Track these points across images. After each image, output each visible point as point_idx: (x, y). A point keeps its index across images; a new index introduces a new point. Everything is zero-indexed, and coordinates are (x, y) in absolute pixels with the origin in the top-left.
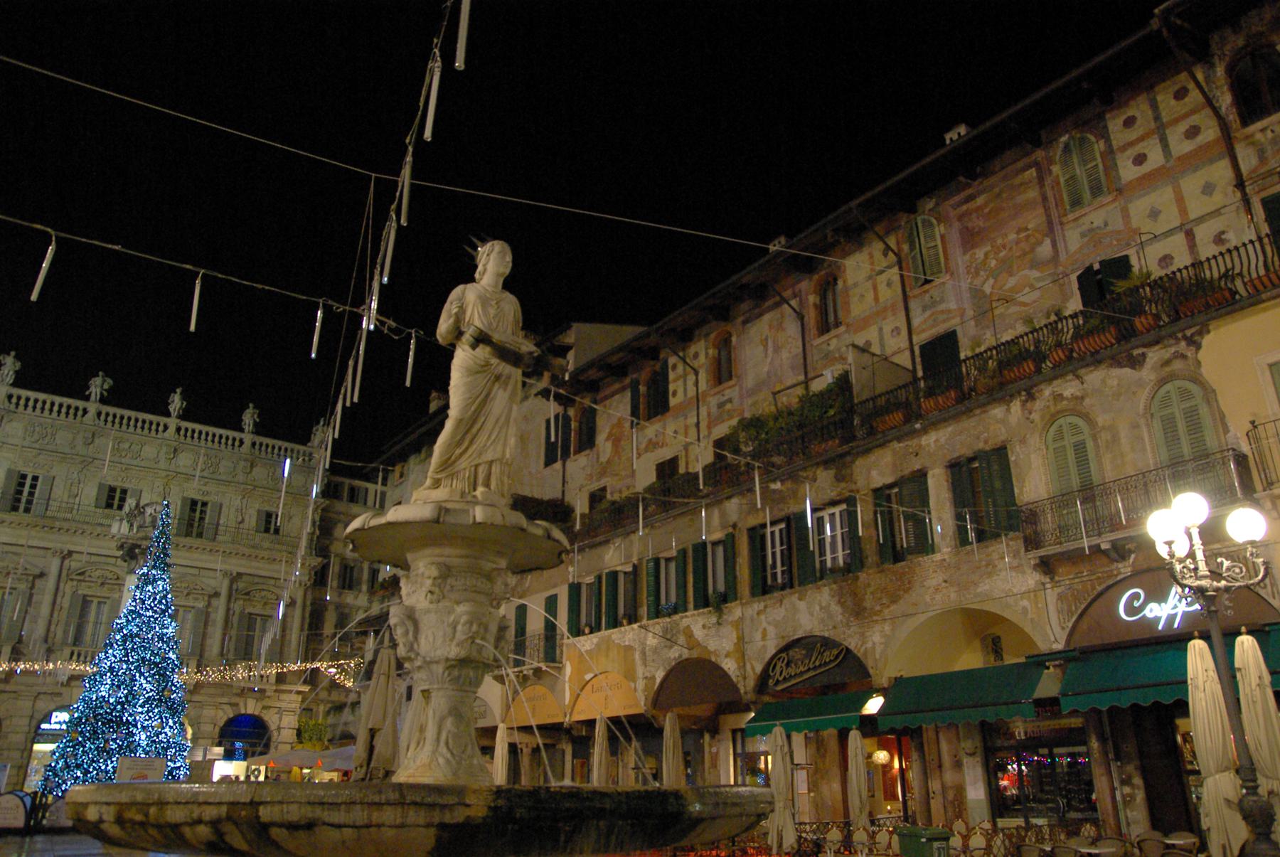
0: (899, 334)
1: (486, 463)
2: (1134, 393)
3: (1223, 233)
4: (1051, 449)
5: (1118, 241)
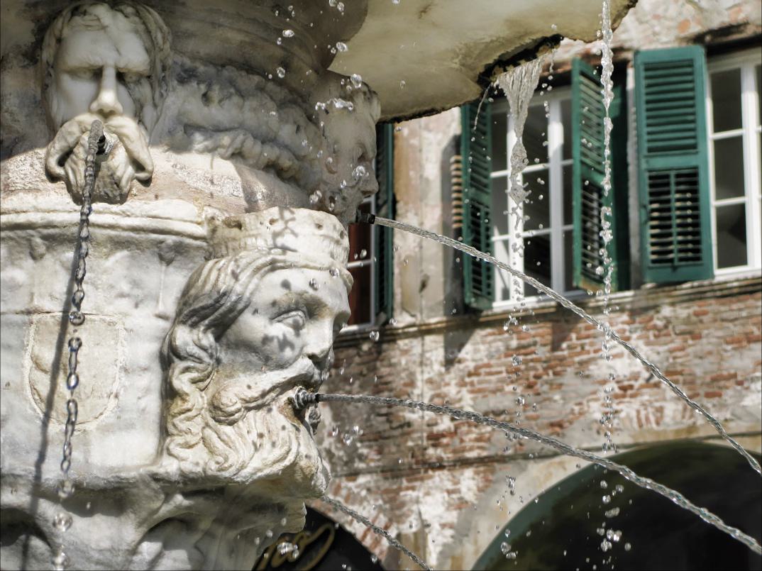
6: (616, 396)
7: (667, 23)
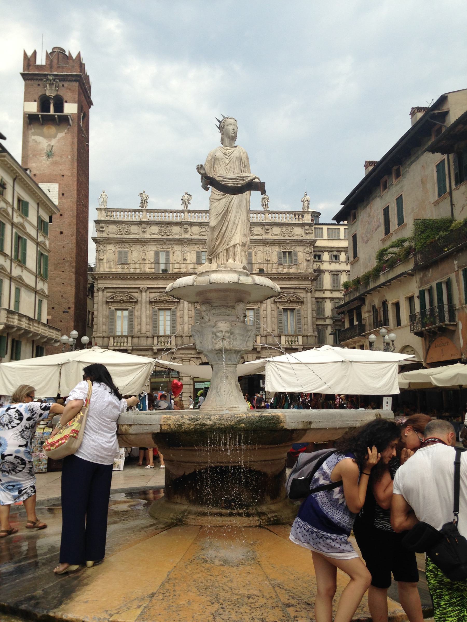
1: (231, 247)
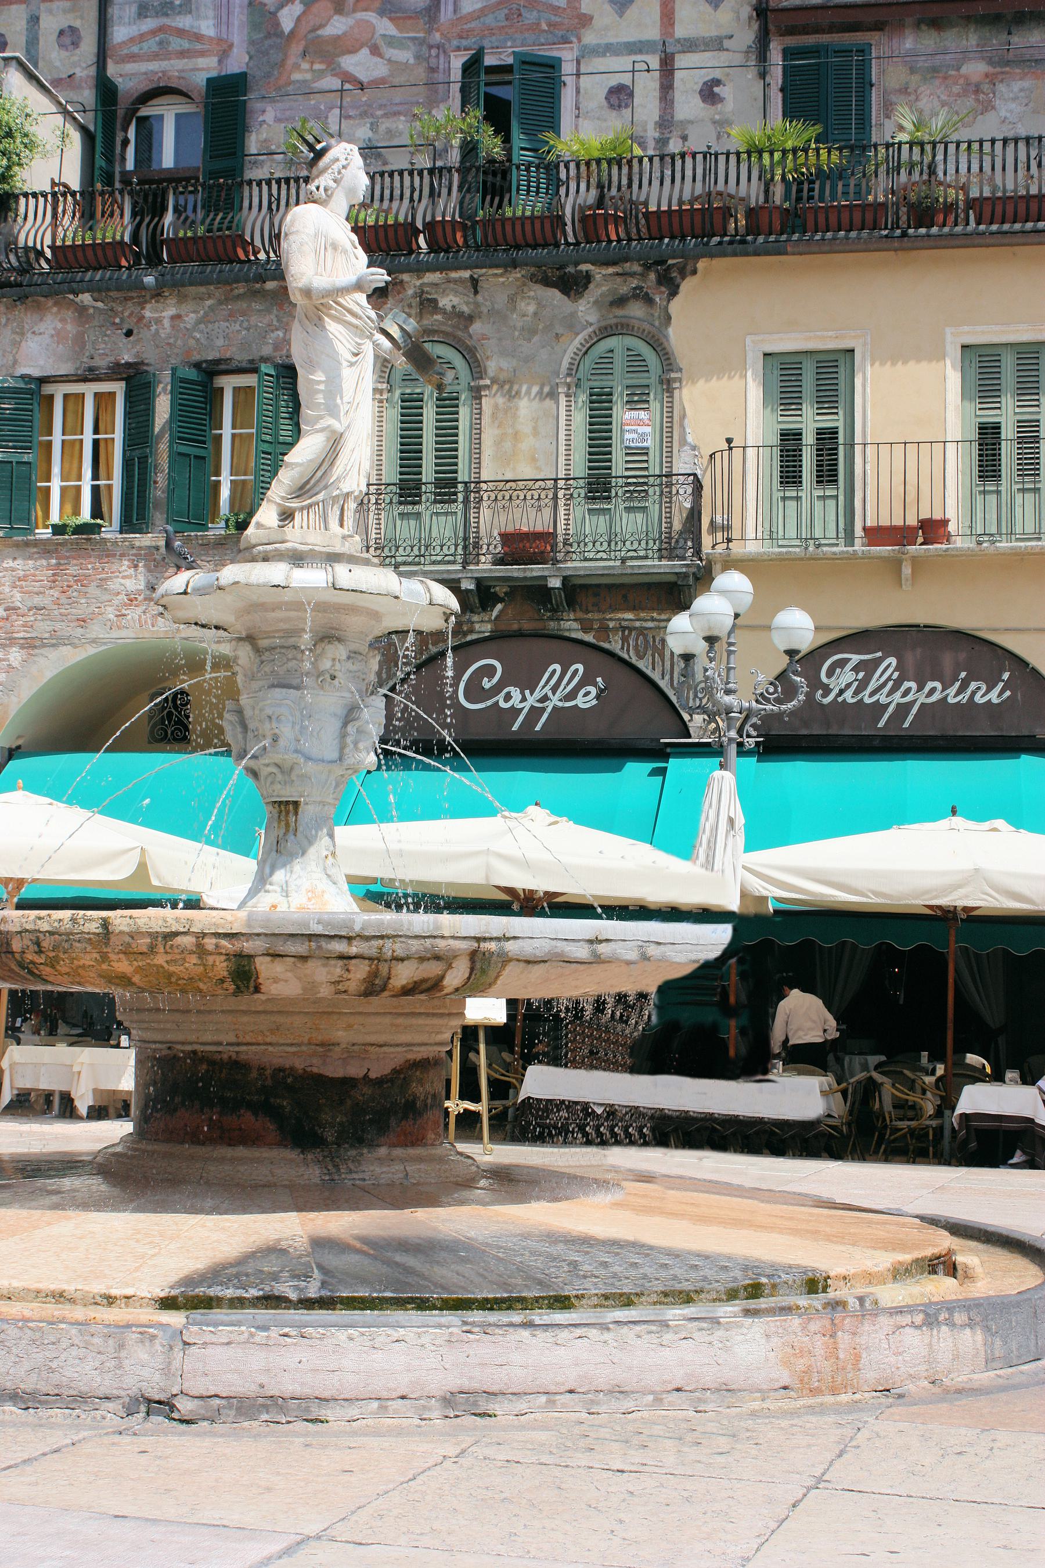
0: (75, 44)
2: (557, 336)
3: (717, 82)
4: (397, 393)
5: (549, 25)
6: (125, 605)
7: (176, 351)
